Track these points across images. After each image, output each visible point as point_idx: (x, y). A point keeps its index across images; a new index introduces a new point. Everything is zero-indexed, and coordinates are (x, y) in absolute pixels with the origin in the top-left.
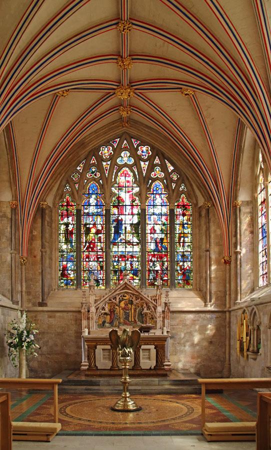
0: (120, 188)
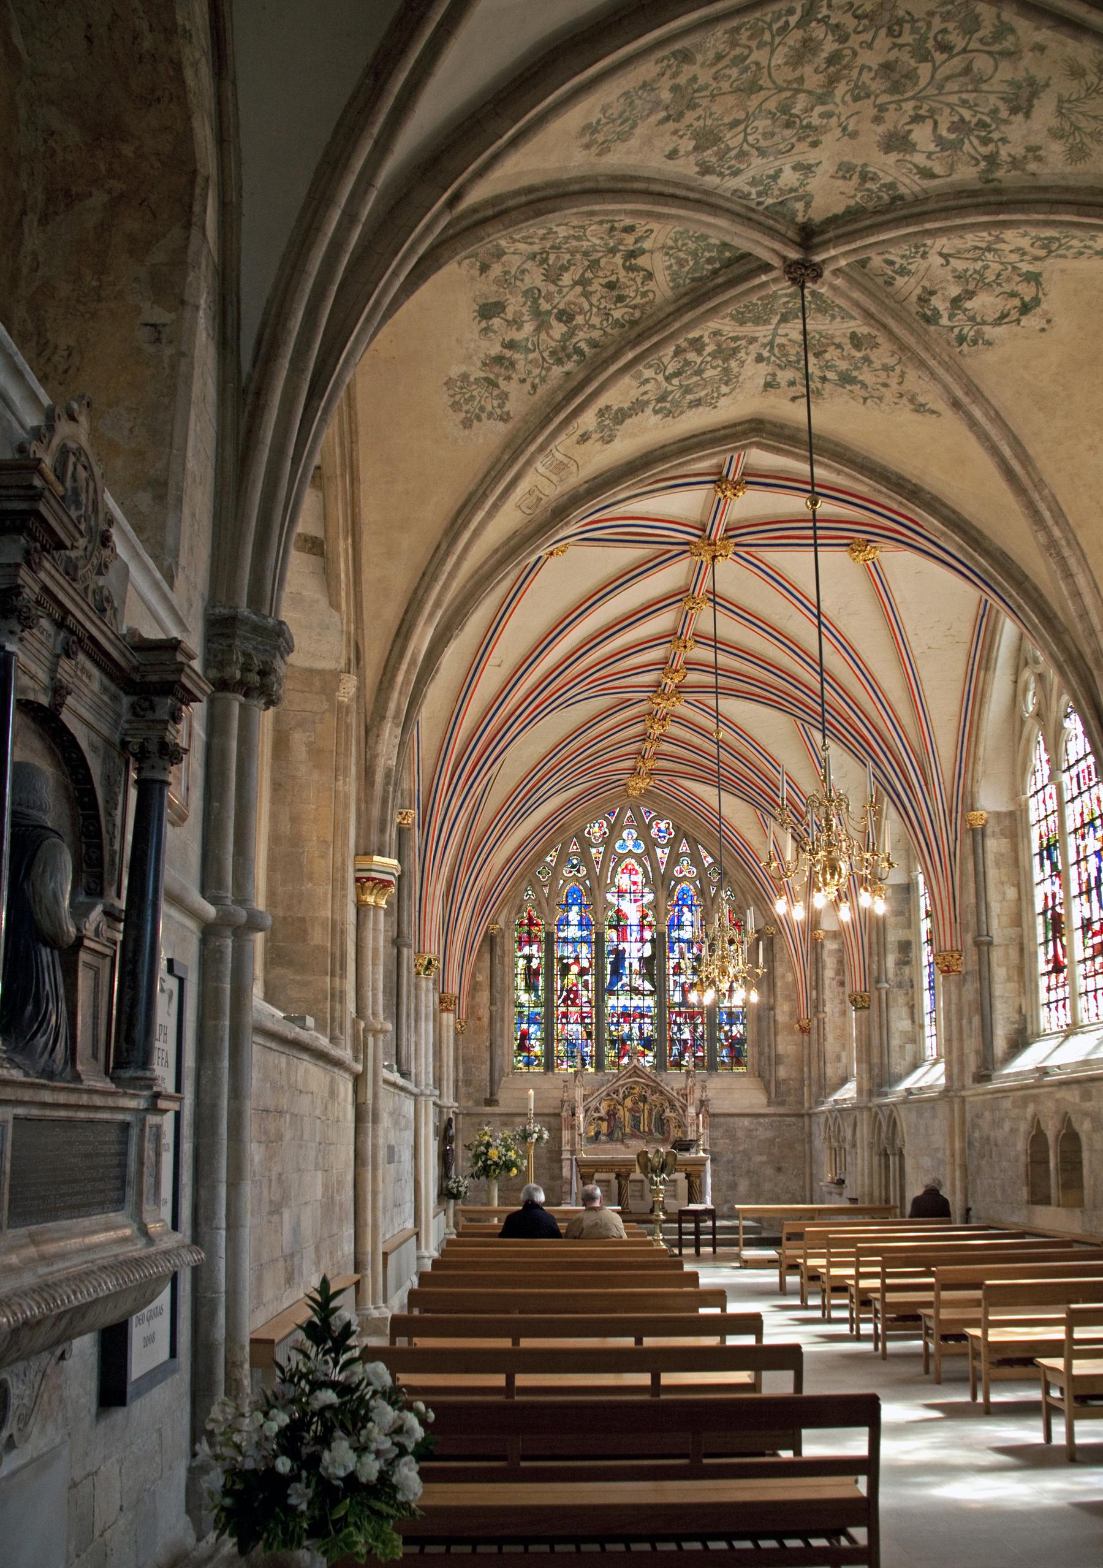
0: (621, 893)
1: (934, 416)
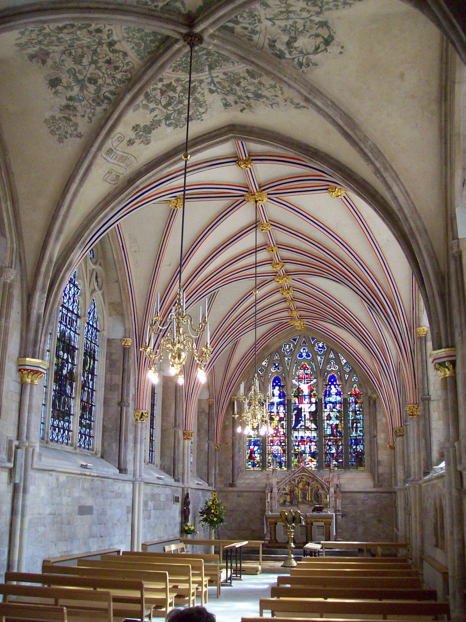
1: (306, 109)
